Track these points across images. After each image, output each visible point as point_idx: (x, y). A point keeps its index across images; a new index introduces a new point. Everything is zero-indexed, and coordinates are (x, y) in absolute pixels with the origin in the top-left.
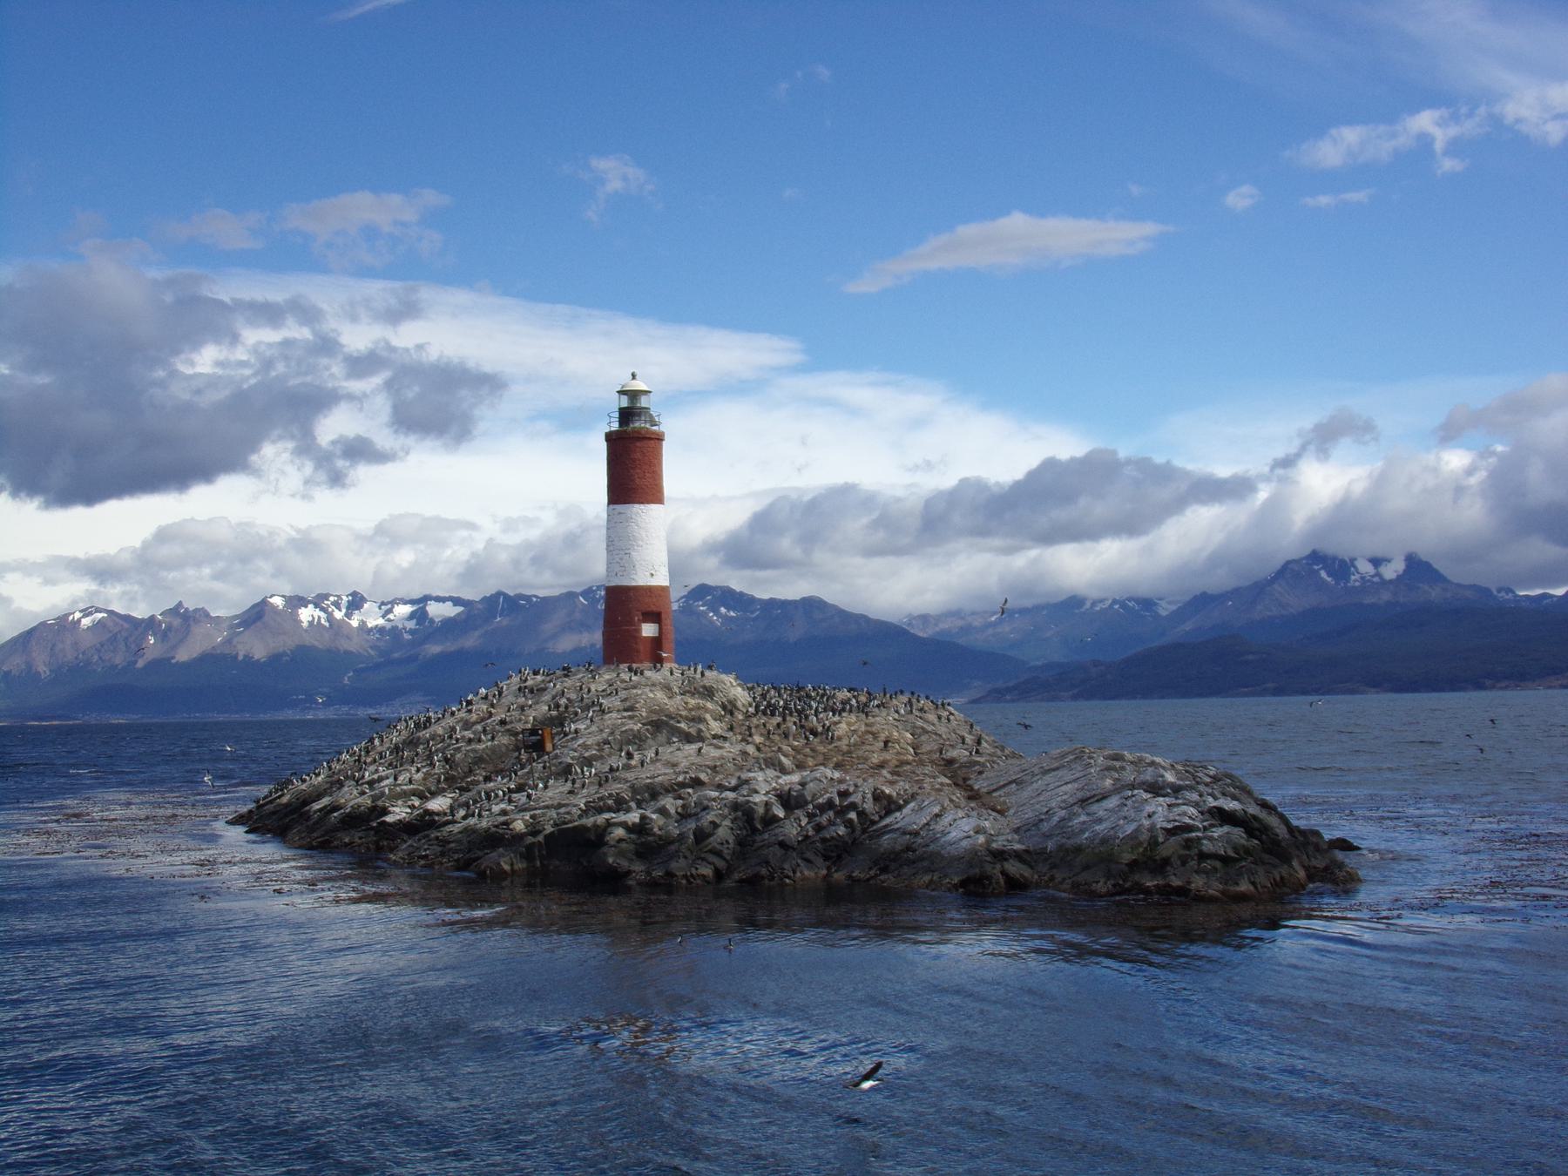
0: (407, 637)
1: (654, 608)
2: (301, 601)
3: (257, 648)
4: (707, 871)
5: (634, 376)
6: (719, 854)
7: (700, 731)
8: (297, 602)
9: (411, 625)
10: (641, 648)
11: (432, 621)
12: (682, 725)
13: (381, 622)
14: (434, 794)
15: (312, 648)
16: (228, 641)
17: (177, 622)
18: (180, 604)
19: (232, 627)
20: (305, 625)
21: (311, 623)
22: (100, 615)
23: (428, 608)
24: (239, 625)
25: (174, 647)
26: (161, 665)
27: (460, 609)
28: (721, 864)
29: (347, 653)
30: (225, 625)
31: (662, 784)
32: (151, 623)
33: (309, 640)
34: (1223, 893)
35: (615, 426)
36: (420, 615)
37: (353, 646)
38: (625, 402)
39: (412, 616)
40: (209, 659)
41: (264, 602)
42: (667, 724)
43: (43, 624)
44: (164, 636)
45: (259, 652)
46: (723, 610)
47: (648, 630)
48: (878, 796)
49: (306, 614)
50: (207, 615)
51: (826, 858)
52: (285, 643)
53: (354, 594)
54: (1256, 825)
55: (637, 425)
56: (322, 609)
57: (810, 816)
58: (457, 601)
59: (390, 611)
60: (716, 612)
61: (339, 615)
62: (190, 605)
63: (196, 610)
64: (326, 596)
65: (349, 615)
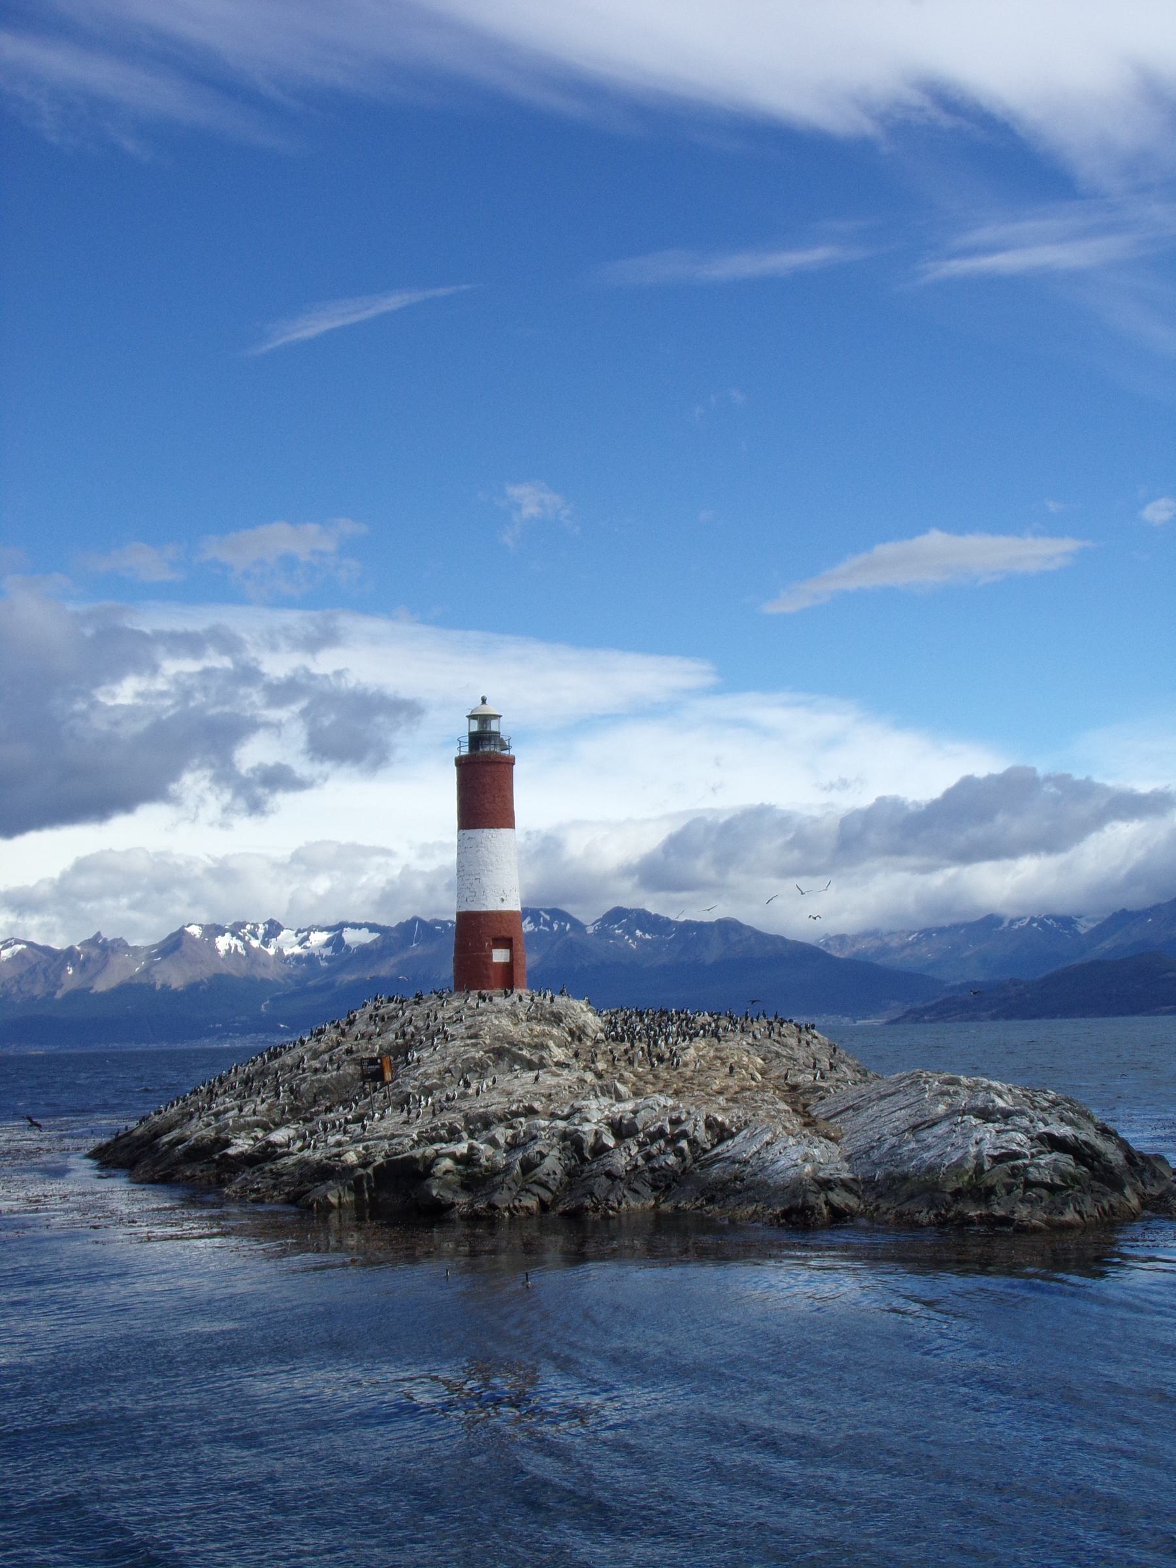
0: (323, 964)
1: (504, 934)
2: (219, 930)
3: (174, 977)
4: (531, 1202)
5: (484, 701)
6: (544, 1185)
7: (542, 1058)
8: (215, 930)
9: (328, 952)
10: (492, 973)
11: (348, 948)
12: (524, 1052)
13: (298, 950)
14: (278, 1126)
15: (229, 976)
16: (146, 971)
17: (95, 953)
18: (98, 935)
19: (150, 957)
20: (222, 953)
21: (228, 952)
22: (19, 947)
23: (344, 935)
25: (92, 978)
26: (79, 995)
27: (376, 935)
28: (547, 1196)
29: (263, 980)
30: (143, 955)
31: (495, 1115)
32: (70, 954)
33: (226, 969)
34: (1047, 1222)
35: (465, 751)
36: (336, 943)
37: (270, 973)
38: (475, 727)
39: (328, 944)
40: (125, 990)
41: (182, 931)
42: (508, 1051)
44: (82, 967)
46: (638, 933)
47: (500, 956)
48: (710, 1124)
49: (223, 943)
50: (126, 946)
51: (655, 1188)
52: (202, 972)
53: (271, 923)
54: (1087, 1151)
55: (487, 749)
56: (239, 938)
57: (641, 1145)
58: (373, 928)
59: (306, 939)
60: (632, 935)
61: (255, 943)
62: (109, 935)
63: (114, 941)
64: (243, 925)
65: (266, 943)
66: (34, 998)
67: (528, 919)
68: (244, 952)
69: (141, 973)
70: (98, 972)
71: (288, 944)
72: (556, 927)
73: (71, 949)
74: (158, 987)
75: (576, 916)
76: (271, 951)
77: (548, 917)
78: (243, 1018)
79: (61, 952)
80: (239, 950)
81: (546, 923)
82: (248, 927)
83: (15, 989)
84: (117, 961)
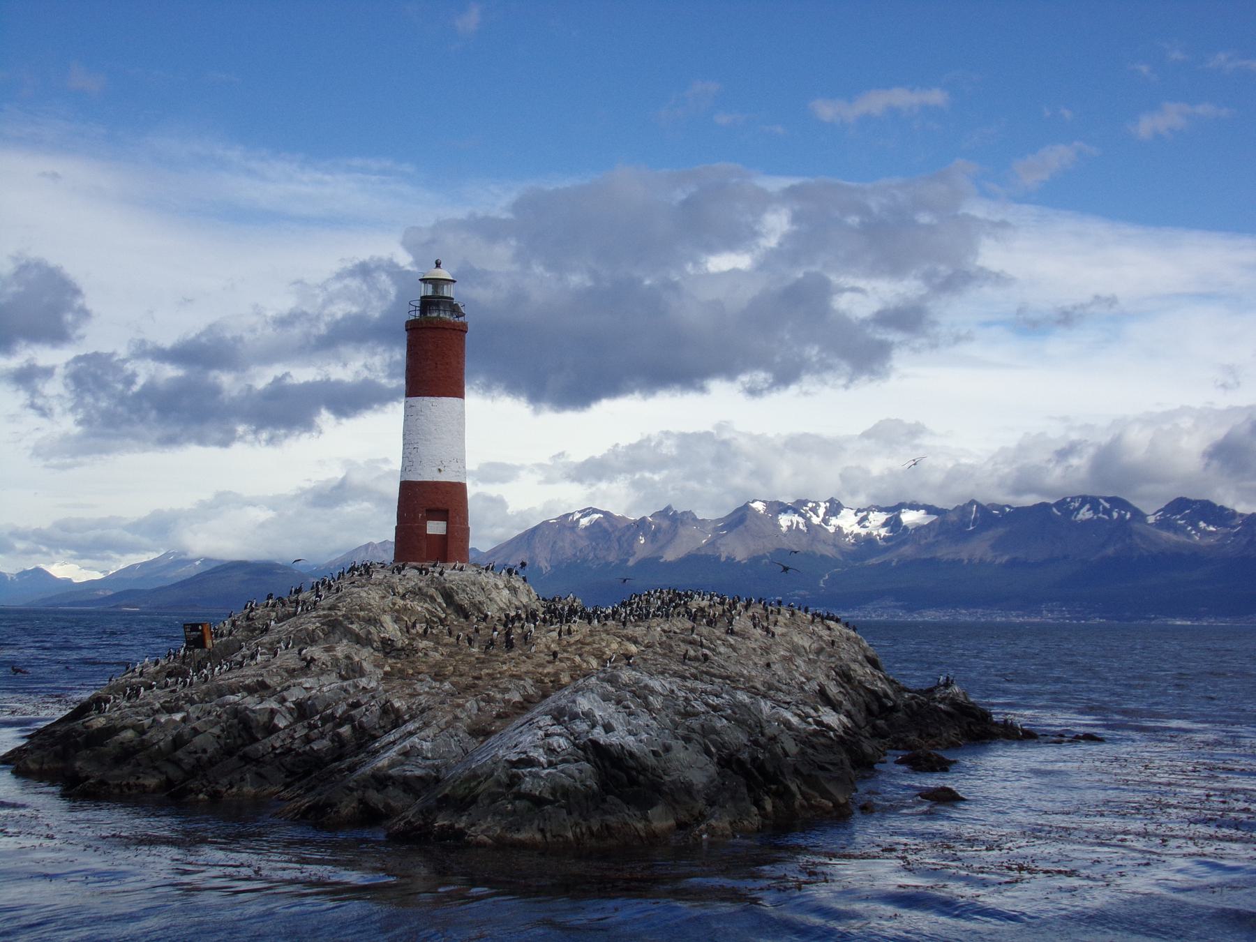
2: (784, 509)
3: (738, 549)
9: (883, 532)
11: (906, 528)
13: (857, 529)
16: (712, 543)
17: (665, 524)
18: (669, 508)
19: (716, 529)
20: (784, 529)
21: (790, 528)
22: (596, 516)
24: (722, 528)
25: (662, 548)
27: (934, 517)
30: (709, 528)
36: (894, 523)
37: (829, 551)
39: (884, 525)
40: (693, 560)
41: (746, 507)
43: (546, 523)
44: (653, 536)
45: (741, 555)
46: (1202, 524)
50: (695, 519)
52: (765, 546)
53: (831, 501)
56: (801, 515)
58: (930, 510)
60: (1196, 527)
61: (816, 520)
62: (680, 508)
63: (684, 513)
64: (805, 503)
66: (608, 564)
67: (1088, 506)
68: (805, 529)
69: (707, 544)
70: (670, 541)
71: (847, 522)
72: (1115, 515)
73: (643, 519)
74: (723, 559)
75: (1136, 503)
76: (831, 529)
77: (1107, 505)
78: (802, 592)
79: (635, 522)
80: (801, 526)
81: (1106, 511)
82: (810, 505)
83: (591, 555)
84: (684, 532)
